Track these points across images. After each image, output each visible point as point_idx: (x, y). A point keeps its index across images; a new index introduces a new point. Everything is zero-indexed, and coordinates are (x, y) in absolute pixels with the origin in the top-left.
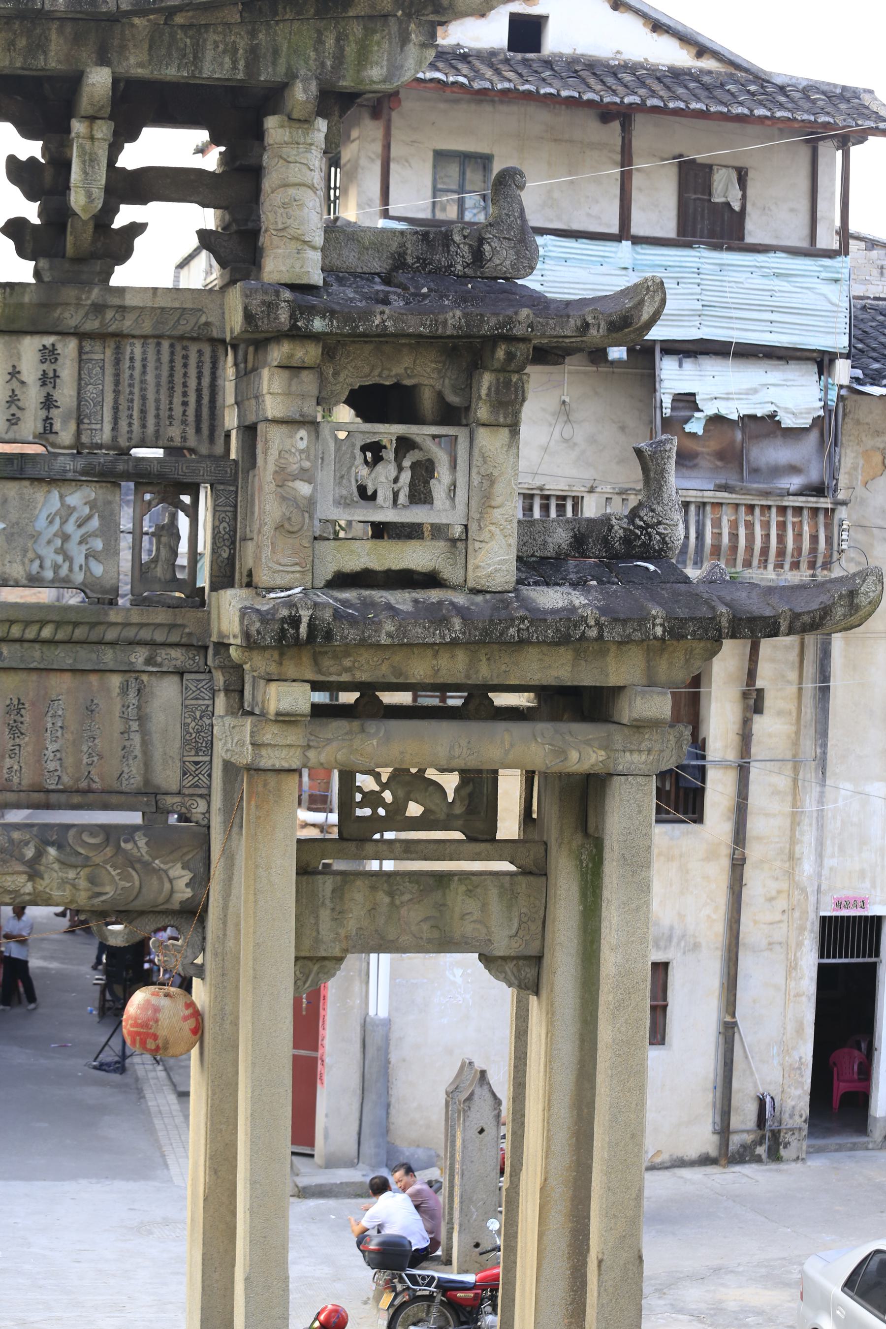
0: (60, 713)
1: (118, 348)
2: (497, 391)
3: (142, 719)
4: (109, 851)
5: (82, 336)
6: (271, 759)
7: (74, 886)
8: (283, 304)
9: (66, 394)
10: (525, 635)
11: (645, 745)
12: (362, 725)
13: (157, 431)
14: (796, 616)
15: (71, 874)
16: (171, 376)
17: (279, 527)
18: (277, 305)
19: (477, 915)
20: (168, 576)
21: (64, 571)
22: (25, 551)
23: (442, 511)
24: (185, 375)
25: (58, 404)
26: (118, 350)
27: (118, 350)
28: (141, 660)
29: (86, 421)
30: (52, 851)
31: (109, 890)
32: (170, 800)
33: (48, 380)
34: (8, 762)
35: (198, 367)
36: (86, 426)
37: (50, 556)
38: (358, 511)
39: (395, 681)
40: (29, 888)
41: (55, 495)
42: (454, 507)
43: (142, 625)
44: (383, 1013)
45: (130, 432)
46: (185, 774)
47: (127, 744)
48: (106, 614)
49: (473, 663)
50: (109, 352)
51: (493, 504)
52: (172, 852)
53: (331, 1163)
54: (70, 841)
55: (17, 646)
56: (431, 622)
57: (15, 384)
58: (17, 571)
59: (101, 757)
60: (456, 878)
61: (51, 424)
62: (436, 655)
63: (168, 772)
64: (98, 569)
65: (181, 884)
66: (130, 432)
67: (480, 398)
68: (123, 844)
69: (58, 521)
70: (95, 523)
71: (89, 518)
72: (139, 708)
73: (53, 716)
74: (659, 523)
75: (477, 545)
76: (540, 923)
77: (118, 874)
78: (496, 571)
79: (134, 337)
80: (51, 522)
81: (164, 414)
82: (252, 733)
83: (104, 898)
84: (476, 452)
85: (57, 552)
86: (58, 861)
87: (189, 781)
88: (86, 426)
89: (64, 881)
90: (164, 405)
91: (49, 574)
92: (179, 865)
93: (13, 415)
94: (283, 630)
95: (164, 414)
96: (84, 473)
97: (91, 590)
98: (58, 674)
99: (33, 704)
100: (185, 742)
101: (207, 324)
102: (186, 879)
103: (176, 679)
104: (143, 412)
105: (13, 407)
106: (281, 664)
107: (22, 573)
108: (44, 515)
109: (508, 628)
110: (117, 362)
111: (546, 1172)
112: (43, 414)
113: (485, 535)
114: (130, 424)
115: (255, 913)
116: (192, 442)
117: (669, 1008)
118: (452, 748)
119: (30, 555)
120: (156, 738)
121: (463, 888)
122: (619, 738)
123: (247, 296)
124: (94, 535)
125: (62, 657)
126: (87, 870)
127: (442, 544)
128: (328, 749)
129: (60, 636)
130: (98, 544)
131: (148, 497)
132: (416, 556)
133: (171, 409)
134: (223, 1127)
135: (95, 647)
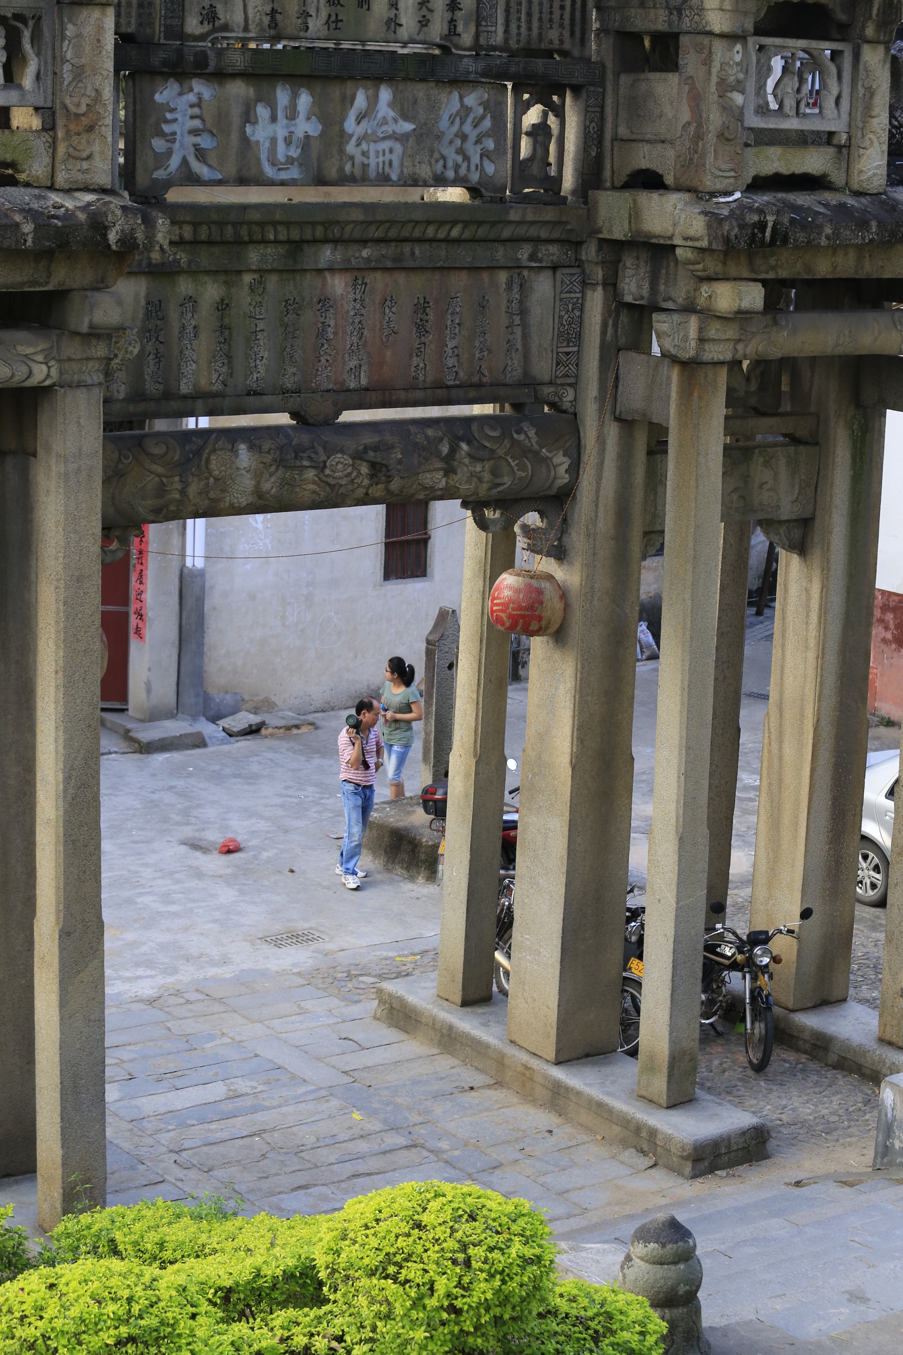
0: (458, 310)
3: (523, 312)
4: (507, 443)
6: (714, 352)
7: (480, 480)
13: (540, 34)
15: (478, 468)
17: (721, 136)
21: (463, 171)
22: (432, 152)
23: (833, 120)
25: (461, 6)
28: (526, 256)
29: (484, 23)
30: (464, 446)
31: (507, 480)
32: (547, 390)
34: (415, 360)
36: (483, 29)
37: (453, 157)
38: (772, 119)
39: (806, 277)
40: (443, 484)
41: (456, 95)
42: (839, 116)
43: (532, 223)
44: (200, 563)
45: (519, 34)
46: (558, 364)
47: (511, 337)
51: (873, 114)
53: (154, 716)
55: (427, 246)
56: (856, 225)
58: (425, 171)
60: (757, 451)
61: (455, 26)
62: (834, 253)
64: (490, 168)
65: (562, 470)
66: (519, 34)
67: (870, 17)
68: (515, 436)
69: (458, 119)
70: (487, 123)
71: (483, 117)
72: (521, 302)
73: (452, 314)
75: (861, 151)
76: (813, 487)
77: (517, 465)
78: (875, 175)
82: (701, 330)
83: (502, 488)
84: (861, 67)
85: (457, 153)
86: (470, 455)
87: (562, 370)
88: (483, 29)
89: (472, 475)
90: (546, 9)
91: (450, 174)
92: (561, 453)
93: (424, 16)
94: (753, 234)
96: (484, 74)
102: (565, 466)
103: (549, 273)
104: (529, 15)
105: (424, 8)
107: (429, 173)
108: (446, 117)
111: (818, 714)
112: (448, 16)
113: (867, 143)
114: (519, 27)
116: (567, 46)
117: (431, 542)
119: (436, 155)
121: (761, 460)
124: (487, 135)
125: (464, 256)
126: (491, 462)
127: (831, 150)
128: (754, 342)
129: (466, 235)
130: (490, 144)
131: (526, 96)
132: (813, 162)
133: (551, 13)
134: (589, 698)
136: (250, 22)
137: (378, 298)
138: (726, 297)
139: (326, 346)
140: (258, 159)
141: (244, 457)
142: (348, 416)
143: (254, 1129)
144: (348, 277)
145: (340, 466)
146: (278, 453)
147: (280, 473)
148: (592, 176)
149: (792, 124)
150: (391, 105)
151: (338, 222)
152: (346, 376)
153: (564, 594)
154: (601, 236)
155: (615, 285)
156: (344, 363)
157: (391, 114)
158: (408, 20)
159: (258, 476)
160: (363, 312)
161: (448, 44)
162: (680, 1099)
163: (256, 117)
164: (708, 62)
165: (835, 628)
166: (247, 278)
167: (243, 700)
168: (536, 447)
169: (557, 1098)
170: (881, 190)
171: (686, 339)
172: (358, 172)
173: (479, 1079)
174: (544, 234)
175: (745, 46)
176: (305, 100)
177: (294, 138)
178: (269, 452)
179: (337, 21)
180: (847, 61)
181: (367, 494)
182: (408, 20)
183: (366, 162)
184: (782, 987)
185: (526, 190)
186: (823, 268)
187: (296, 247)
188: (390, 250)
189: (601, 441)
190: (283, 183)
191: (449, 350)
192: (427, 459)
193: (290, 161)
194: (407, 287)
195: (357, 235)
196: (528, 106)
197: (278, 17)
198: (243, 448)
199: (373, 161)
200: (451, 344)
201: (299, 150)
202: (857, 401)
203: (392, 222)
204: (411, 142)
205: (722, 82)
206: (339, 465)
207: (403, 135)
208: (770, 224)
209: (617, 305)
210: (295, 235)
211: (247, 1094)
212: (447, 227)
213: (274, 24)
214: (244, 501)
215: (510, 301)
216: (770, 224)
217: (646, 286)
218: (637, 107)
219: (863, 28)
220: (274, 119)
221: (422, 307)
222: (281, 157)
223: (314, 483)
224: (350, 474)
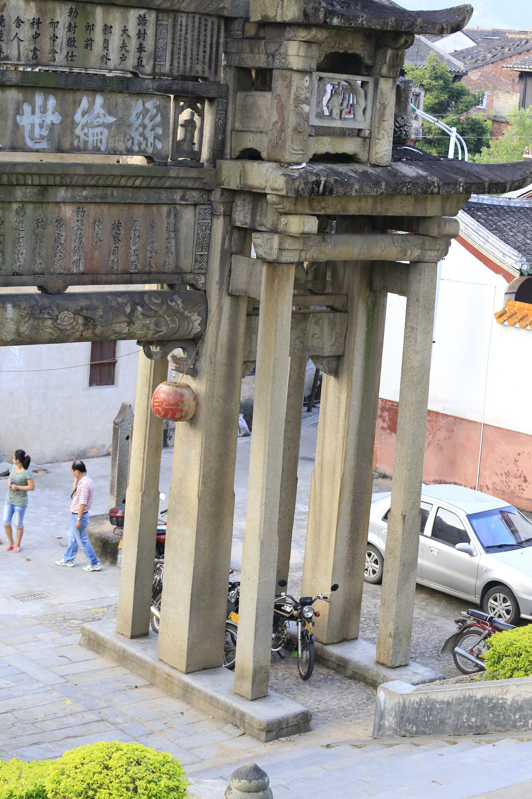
0: (138, 228)
1: (175, 18)
2: (393, 60)
3: (176, 231)
4: (165, 307)
5: (159, 10)
6: (287, 257)
7: (148, 328)
8: (322, 9)
9: (149, 44)
10: (409, 191)
11: (437, 247)
12: (323, 238)
13: (191, 67)
14: (514, 182)
15: (148, 322)
16: (199, 35)
17: (295, 130)
18: (319, 10)
19: (319, 334)
20: (190, 150)
21: (143, 147)
22: (125, 135)
23: (361, 123)
24: (205, 35)
25: (145, 49)
26: (175, 20)
27: (175, 20)
28: (179, 197)
29: (158, 60)
30: (139, 308)
31: (164, 329)
33: (141, 35)
35: (211, 31)
36: (158, 63)
38: (326, 121)
39: (343, 214)
40: (126, 330)
41: (140, 102)
42: (365, 120)
43: (184, 178)
45: (179, 67)
48: (169, 172)
49: (375, 203)
50: (170, 20)
51: (385, 119)
52: (193, 307)
54: (147, 302)
55: (121, 190)
56: (373, 184)
57: (125, 36)
58: (121, 146)
59: (156, 253)
60: (311, 315)
61: (141, 61)
62: (360, 200)
63: (187, 261)
64: (159, 145)
65: (196, 324)
66: (179, 67)
67: (385, 63)
68: (170, 303)
69: (141, 116)
70: (158, 119)
71: (156, 115)
72: (175, 225)
73: (135, 230)
74: (405, 125)
75: (377, 141)
78: (385, 155)
79: (182, 12)
80: (138, 118)
81: (195, 57)
82: (280, 243)
83: (161, 334)
84: (379, 91)
85: (140, 135)
86: (143, 314)
87: (198, 265)
88: (158, 63)
89: (144, 325)
90: (195, 53)
92: (196, 314)
93: (123, 55)
94: (313, 188)
95: (195, 57)
96: (158, 90)
97: (157, 158)
98: (138, 206)
99: (125, 223)
100: (198, 244)
101: (223, 8)
102: (199, 322)
103: (192, 208)
104: (185, 55)
106: (295, 205)
107: (124, 147)
108: (134, 114)
109: (403, 187)
110: (174, 26)
111: (344, 470)
112: (137, 55)
113: (381, 136)
114: (179, 63)
115: (275, 342)
116: (207, 74)
117: (117, 365)
118: (361, 249)
119: (128, 137)
120: (182, 241)
121: (314, 320)
122: (428, 243)
123: (305, 3)
124: (158, 125)
126: (155, 318)
127: (360, 140)
129: (144, 184)
130: (160, 131)
131: (182, 103)
132: (349, 146)
133: (198, 55)
134: (209, 458)
135: (158, 190)
136: (21, 55)
137: (91, 220)
138: (296, 224)
139: (60, 247)
140: (23, 137)
141: (10, 311)
142: (72, 289)
143: (8, 709)
144: (74, 207)
145: (66, 319)
146: (30, 310)
147: (31, 322)
148: (219, 152)
149: (337, 124)
150: (102, 106)
151: (69, 175)
152: (71, 265)
153: (196, 398)
154: (223, 187)
155: (230, 216)
156: (70, 258)
157: (102, 111)
158: (114, 56)
159: (18, 323)
160: (82, 228)
161: (137, 72)
162: (259, 695)
163: (23, 111)
164: (289, 86)
165: (355, 420)
166: (15, 206)
167: (5, 455)
168: (182, 310)
169: (187, 694)
170: (388, 164)
171: (271, 248)
172: (82, 146)
173: (141, 682)
174: (190, 185)
175: (311, 77)
176: (52, 102)
177: (45, 124)
178: (25, 309)
179: (72, 56)
180: (370, 88)
181: (82, 335)
182: (114, 56)
183: (87, 139)
184: (320, 630)
185: (180, 159)
186: (353, 209)
187: (44, 188)
188: (99, 192)
189: (220, 307)
190: (37, 151)
191: (132, 252)
192: (117, 316)
193: (42, 137)
194: (110, 214)
195: (80, 182)
196: (182, 109)
197: (38, 52)
198: (9, 306)
199: (90, 139)
200: (133, 248)
201: (48, 132)
202: (370, 287)
203: (101, 176)
204: (114, 128)
205: (297, 98)
206: (66, 318)
207: (108, 124)
208: (323, 183)
209: (232, 228)
210: (44, 181)
211: (4, 688)
212: (133, 179)
213: (35, 57)
214: (9, 338)
215: (169, 224)
216: (323, 183)
217: (249, 217)
218: (246, 112)
219: (381, 69)
220: (33, 112)
221: (117, 226)
222: (37, 135)
223: (51, 328)
224: (72, 323)
